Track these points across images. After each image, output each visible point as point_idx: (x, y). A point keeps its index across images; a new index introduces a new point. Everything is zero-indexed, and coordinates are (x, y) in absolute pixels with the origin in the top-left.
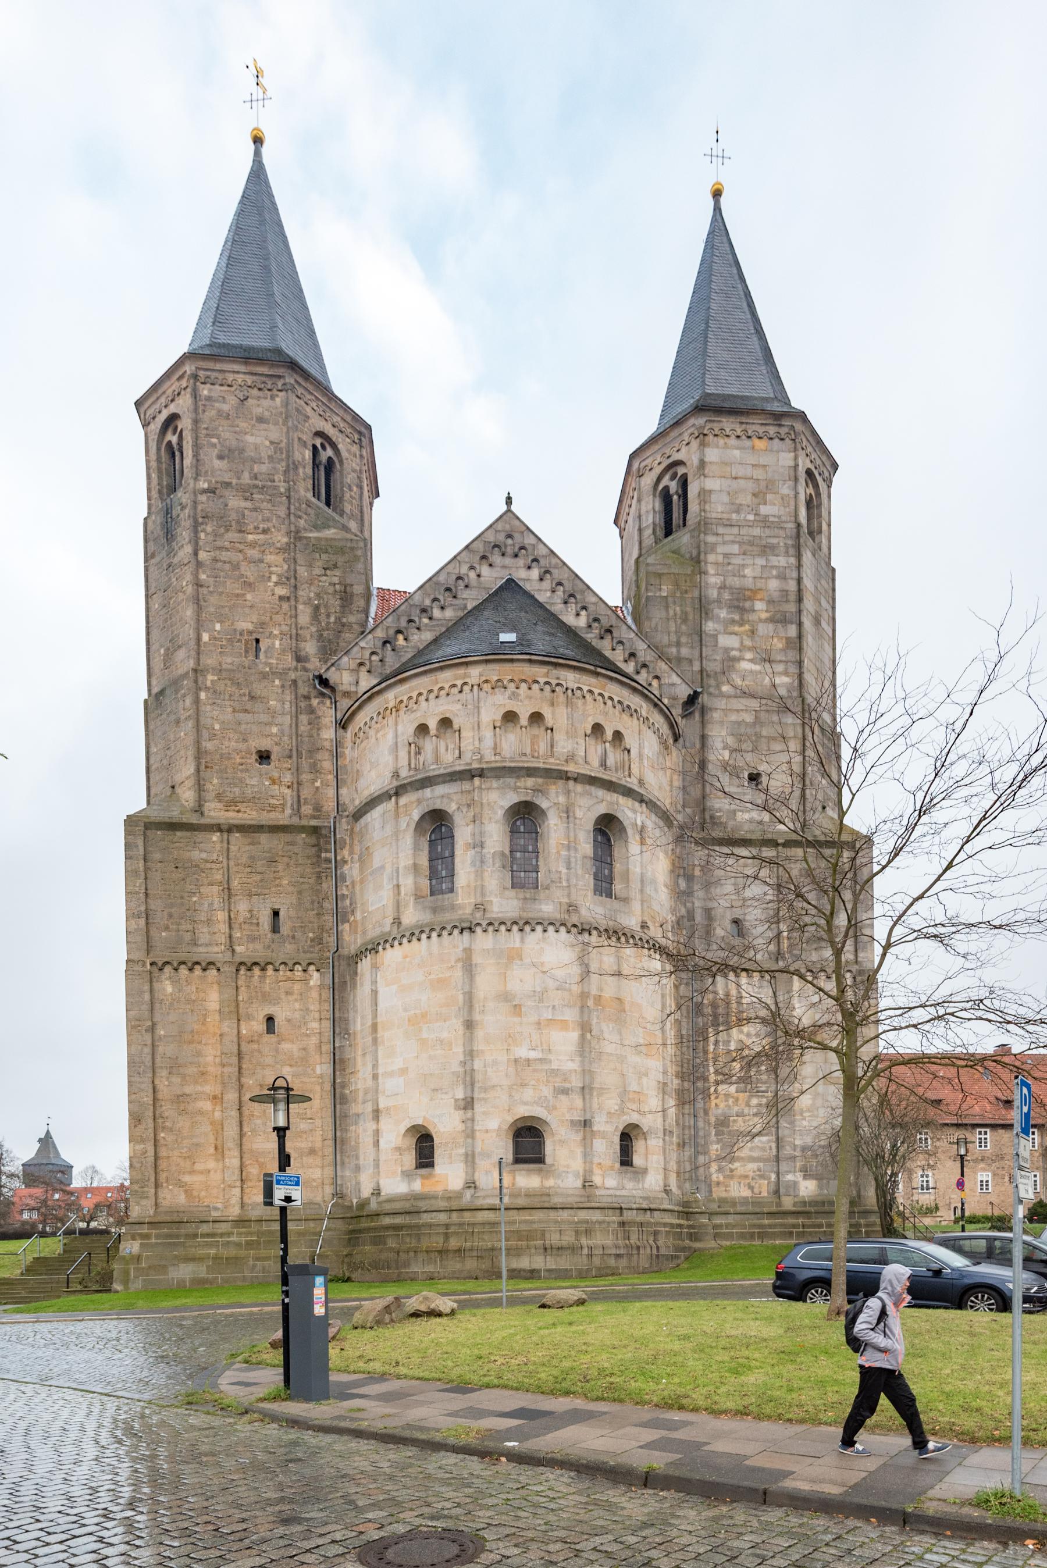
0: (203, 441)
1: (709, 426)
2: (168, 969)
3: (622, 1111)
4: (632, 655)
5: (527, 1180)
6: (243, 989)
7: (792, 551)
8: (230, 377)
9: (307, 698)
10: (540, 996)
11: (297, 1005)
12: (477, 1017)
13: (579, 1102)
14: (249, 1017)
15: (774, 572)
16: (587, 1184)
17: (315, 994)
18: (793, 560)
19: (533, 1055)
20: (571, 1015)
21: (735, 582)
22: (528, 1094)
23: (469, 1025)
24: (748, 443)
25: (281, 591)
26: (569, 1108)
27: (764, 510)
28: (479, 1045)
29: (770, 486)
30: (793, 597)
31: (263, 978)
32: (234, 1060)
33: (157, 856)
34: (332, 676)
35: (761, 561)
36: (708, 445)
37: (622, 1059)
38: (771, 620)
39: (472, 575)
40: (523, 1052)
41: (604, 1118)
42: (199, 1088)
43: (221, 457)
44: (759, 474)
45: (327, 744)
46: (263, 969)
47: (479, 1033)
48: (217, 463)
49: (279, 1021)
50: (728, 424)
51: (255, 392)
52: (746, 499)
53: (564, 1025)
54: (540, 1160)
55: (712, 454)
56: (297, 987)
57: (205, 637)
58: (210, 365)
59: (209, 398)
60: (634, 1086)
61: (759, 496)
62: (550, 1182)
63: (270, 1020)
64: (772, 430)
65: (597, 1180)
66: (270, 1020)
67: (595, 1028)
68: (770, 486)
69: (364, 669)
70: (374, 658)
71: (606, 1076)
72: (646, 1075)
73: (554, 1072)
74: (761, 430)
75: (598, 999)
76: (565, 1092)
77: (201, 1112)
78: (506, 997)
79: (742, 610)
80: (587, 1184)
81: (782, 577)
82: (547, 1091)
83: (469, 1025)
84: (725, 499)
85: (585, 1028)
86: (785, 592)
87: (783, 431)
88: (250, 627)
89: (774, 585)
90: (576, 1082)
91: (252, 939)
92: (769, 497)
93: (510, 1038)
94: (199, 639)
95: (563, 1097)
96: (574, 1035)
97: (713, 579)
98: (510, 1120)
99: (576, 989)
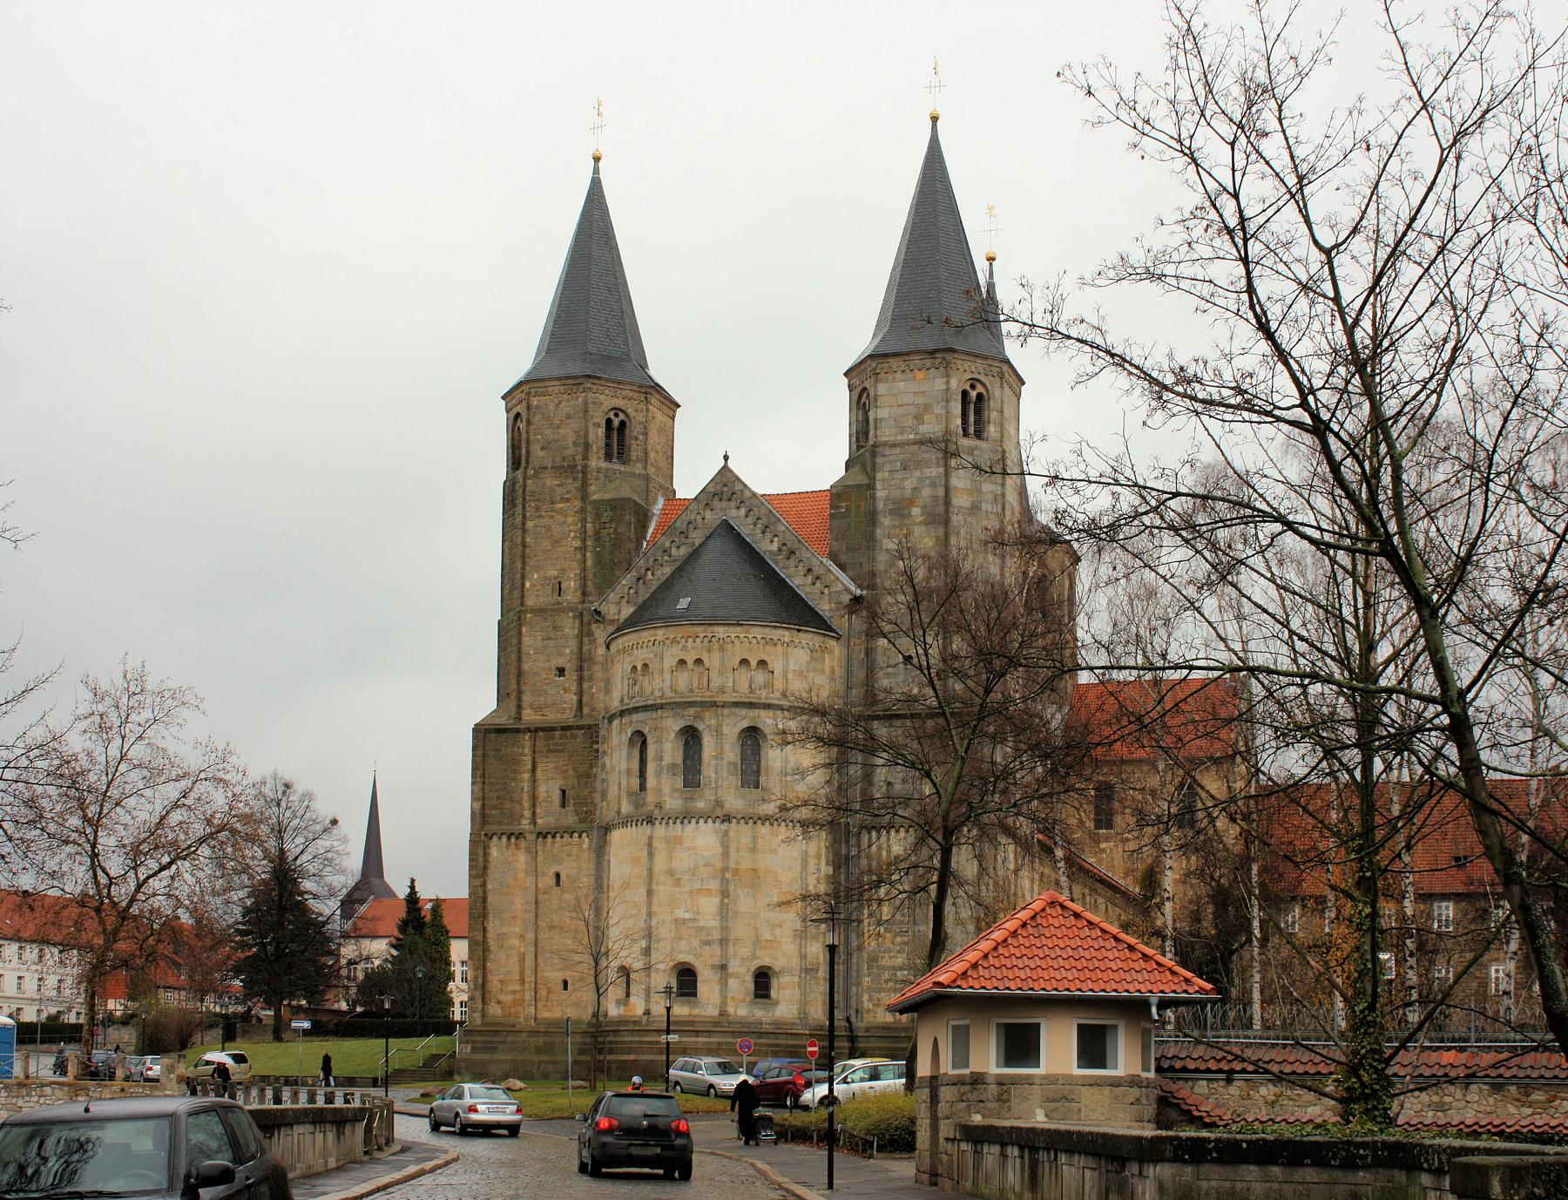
0: (532, 438)
1: (880, 366)
2: (495, 838)
3: (755, 957)
4: (809, 570)
5: (681, 1010)
6: (540, 853)
7: (941, 462)
8: (550, 389)
9: (589, 624)
10: (693, 871)
11: (574, 864)
12: (654, 887)
13: (717, 950)
14: (544, 874)
15: (927, 482)
16: (723, 1013)
17: (586, 855)
18: (941, 470)
19: (687, 916)
20: (714, 885)
21: (897, 494)
22: (683, 945)
23: (650, 893)
24: (910, 375)
25: (577, 544)
26: (712, 955)
27: (923, 429)
28: (655, 909)
29: (927, 408)
30: (941, 501)
31: (553, 843)
32: (533, 907)
33: (492, 753)
34: (603, 609)
35: (918, 474)
36: (881, 381)
37: (755, 916)
38: (925, 523)
39: (699, 517)
40: (681, 914)
41: (738, 962)
42: (511, 929)
43: (543, 449)
44: (920, 400)
45: (600, 659)
46: (554, 837)
47: (655, 900)
48: (542, 453)
49: (563, 877)
50: (894, 363)
51: (566, 396)
52: (909, 422)
53: (709, 893)
54: (695, 995)
55: (882, 388)
56: (575, 850)
57: (528, 585)
58: (538, 384)
59: (537, 407)
60: (767, 936)
61: (919, 418)
62: (695, 1012)
63: (558, 876)
64: (928, 362)
65: (731, 1010)
66: (558, 876)
67: (732, 895)
68: (927, 408)
69: (624, 600)
70: (632, 591)
71: (740, 930)
72: (781, 926)
73: (701, 929)
74: (919, 363)
75: (736, 872)
76: (707, 943)
77: (512, 948)
78: (671, 872)
79: (903, 516)
80: (723, 1013)
81: (933, 485)
82: (695, 943)
83: (650, 893)
84: (891, 422)
85: (725, 894)
86: (934, 498)
87: (937, 362)
88: (555, 573)
89: (926, 492)
90: (716, 936)
91: (548, 813)
92: (926, 417)
93: (673, 903)
94: (523, 585)
95: (707, 947)
96: (716, 900)
97: (880, 494)
98: (672, 964)
99: (719, 865)
